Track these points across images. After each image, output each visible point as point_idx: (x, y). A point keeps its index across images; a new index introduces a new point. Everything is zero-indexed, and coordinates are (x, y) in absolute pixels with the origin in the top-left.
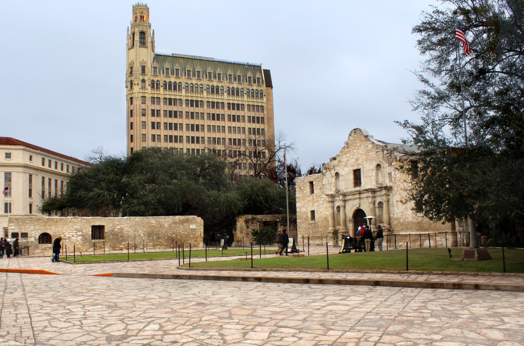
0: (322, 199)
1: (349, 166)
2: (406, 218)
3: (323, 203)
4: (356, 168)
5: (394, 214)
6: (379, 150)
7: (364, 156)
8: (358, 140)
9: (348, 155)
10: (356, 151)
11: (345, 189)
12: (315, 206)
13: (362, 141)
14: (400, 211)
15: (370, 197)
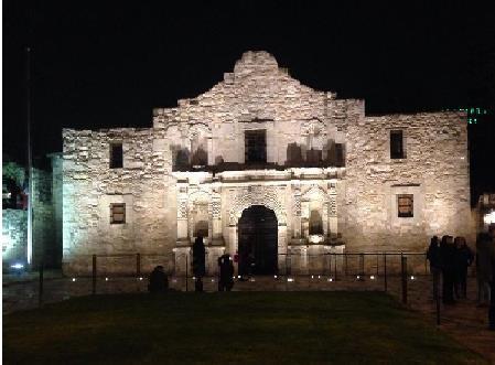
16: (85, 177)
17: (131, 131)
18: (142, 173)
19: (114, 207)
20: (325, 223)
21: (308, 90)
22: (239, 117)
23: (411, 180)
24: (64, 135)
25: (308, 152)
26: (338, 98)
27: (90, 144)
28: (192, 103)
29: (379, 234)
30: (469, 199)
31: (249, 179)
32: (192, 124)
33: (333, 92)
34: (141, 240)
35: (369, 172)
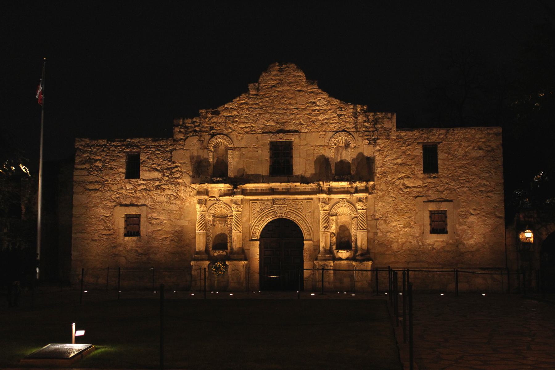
5: (376, 234)
6: (344, 113)
16: (97, 187)
17: (149, 142)
18: (157, 183)
19: (128, 218)
20: (353, 238)
21: (336, 102)
22: (262, 129)
23: (443, 196)
24: (77, 145)
25: (337, 164)
26: (369, 110)
27: (104, 154)
28: (213, 113)
29: (409, 250)
30: (503, 215)
31: (272, 191)
32: (213, 136)
33: (362, 104)
34: (156, 254)
35: (401, 186)
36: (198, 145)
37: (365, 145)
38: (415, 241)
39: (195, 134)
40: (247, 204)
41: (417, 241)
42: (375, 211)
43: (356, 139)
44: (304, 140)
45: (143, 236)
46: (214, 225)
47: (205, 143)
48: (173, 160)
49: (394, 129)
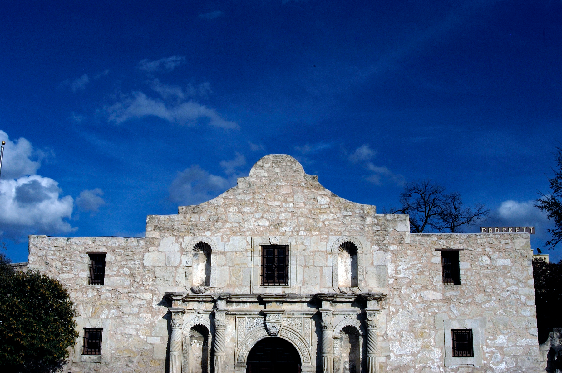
0: (137, 302)
1: (248, 233)
2: (425, 367)
3: (139, 313)
4: (276, 241)
5: (388, 357)
6: (351, 214)
7: (302, 219)
8: (287, 181)
9: (246, 209)
10: (277, 203)
11: (229, 286)
12: (103, 316)
13: (299, 185)
14: (408, 349)
15: (327, 312)
36: (177, 247)
37: (375, 251)
38: (436, 366)
39: (173, 234)
40: (232, 319)
41: (438, 367)
42: (387, 330)
43: (364, 246)
44: (303, 244)
45: (104, 355)
46: (192, 345)
47: (183, 246)
48: (146, 264)
49: (408, 233)
